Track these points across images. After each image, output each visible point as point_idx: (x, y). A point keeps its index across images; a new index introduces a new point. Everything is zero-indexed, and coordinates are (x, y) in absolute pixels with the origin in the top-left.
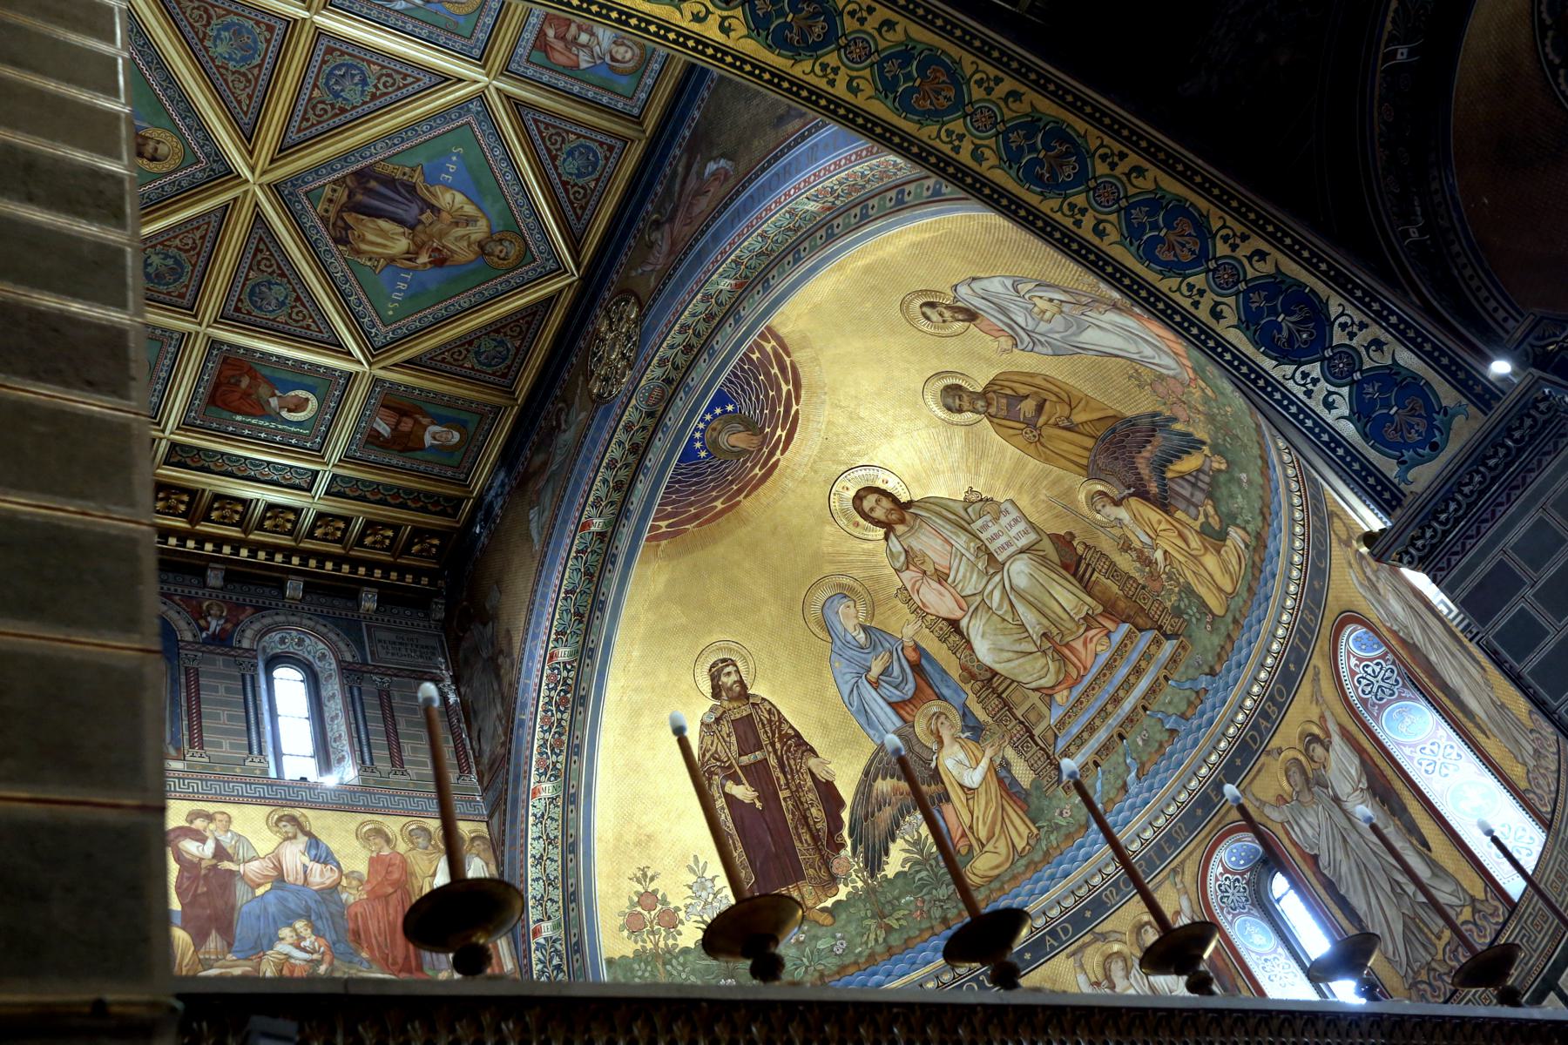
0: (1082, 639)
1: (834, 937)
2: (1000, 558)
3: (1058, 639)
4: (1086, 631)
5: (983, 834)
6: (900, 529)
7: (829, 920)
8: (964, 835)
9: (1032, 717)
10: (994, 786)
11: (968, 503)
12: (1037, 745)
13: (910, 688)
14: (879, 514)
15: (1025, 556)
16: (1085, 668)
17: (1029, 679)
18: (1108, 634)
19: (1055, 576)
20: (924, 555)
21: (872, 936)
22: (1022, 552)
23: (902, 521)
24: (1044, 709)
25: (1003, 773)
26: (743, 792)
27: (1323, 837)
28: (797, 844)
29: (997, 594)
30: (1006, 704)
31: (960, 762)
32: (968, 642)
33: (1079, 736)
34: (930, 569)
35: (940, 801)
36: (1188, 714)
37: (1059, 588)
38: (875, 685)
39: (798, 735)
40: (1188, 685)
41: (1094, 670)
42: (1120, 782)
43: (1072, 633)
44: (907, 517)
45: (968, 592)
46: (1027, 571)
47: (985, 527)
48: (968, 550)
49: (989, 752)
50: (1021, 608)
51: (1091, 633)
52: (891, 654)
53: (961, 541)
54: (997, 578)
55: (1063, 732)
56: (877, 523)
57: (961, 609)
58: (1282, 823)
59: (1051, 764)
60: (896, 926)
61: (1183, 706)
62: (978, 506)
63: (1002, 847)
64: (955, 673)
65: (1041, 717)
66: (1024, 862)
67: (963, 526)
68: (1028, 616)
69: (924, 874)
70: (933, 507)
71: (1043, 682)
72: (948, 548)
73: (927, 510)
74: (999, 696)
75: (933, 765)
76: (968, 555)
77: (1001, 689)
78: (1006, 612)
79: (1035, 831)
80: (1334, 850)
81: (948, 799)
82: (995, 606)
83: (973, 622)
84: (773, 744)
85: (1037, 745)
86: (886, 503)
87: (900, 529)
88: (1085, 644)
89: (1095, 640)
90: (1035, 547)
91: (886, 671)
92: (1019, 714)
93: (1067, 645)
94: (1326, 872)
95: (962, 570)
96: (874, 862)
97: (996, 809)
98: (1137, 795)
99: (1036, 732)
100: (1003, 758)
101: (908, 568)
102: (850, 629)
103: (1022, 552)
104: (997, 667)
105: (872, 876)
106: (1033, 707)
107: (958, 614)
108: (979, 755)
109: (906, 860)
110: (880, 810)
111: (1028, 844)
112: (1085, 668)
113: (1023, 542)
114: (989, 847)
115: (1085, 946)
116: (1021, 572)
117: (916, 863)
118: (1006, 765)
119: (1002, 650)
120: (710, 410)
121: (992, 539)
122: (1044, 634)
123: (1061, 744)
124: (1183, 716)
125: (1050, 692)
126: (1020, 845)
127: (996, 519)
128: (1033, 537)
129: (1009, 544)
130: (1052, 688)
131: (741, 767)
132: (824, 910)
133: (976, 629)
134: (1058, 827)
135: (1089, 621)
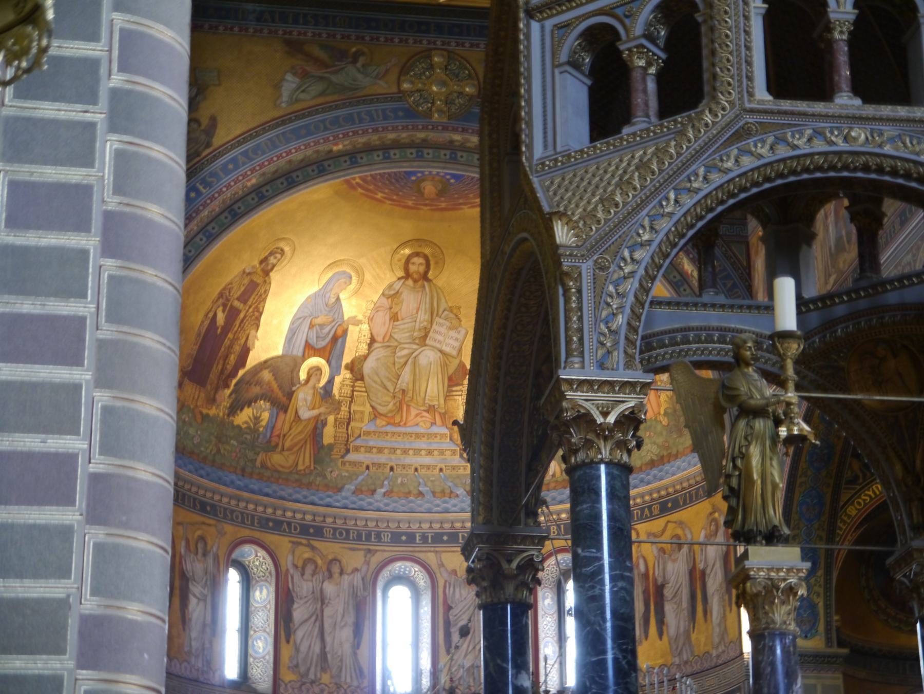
0: (418, 412)
1: (197, 432)
2: (428, 342)
3: (407, 399)
4: (424, 411)
5: (288, 444)
6: (410, 282)
7: (199, 420)
8: (279, 436)
9: (357, 416)
10: (310, 427)
12: (347, 429)
13: (322, 344)
14: (412, 268)
15: (439, 354)
16: (405, 424)
17: (374, 399)
18: (433, 424)
19: (440, 376)
20: (402, 302)
21: (211, 447)
22: (441, 351)
23: (415, 281)
24: (366, 419)
25: (319, 426)
26: (221, 318)
27: (464, 604)
28: (215, 366)
29: (405, 352)
30: (352, 397)
31: (306, 400)
32: (368, 354)
33: (371, 448)
34: (395, 310)
35: (282, 409)
36: (437, 495)
37: (436, 383)
38: (311, 326)
39: (261, 314)
40: (450, 484)
41: (409, 430)
42: (373, 487)
43: (417, 404)
44: (420, 283)
45: (396, 336)
46: (432, 359)
47: (441, 325)
48: (420, 323)
49: (322, 410)
50: (408, 369)
51: (425, 414)
52: (333, 321)
53: (423, 316)
54: (415, 347)
55: (365, 438)
56: (406, 270)
57: (384, 338)
58: (446, 581)
59: (346, 445)
60: (222, 451)
61: (438, 489)
62: (451, 315)
63: (292, 459)
64: (347, 359)
65: (362, 420)
66: (296, 476)
67: (433, 313)
68: (406, 374)
69: (249, 437)
70: (435, 295)
71: (379, 408)
72: (415, 312)
73: (431, 291)
74: (353, 391)
75: (294, 388)
76: (417, 324)
77: (357, 389)
78: (400, 363)
79: (312, 468)
80: (464, 613)
81: (286, 412)
82: (399, 354)
83: (381, 349)
84: (250, 307)
85: (347, 429)
86: (422, 269)
87: (410, 282)
88: (417, 415)
89: (424, 419)
90: (449, 358)
91: (322, 326)
92: (353, 407)
93: (408, 406)
94: (451, 617)
95: (406, 326)
96: (235, 408)
97: (300, 441)
98: (377, 501)
99: (352, 424)
100: (326, 419)
101: (388, 298)
102: (333, 292)
103: (441, 351)
104: (366, 378)
105: (229, 415)
106: (362, 412)
107: (379, 338)
108: (317, 406)
109: (246, 422)
110: (255, 385)
111: (304, 470)
112: (405, 424)
113: (447, 349)
114: (286, 453)
115: (300, 544)
116: (428, 357)
117: (249, 428)
118: (324, 424)
119: (377, 374)
120: (447, 174)
121: (436, 332)
122: (404, 391)
123: (358, 443)
124: (434, 493)
125: (378, 415)
126: (300, 467)
127: (450, 328)
128: (454, 353)
129: (440, 342)
130: (381, 414)
131: (231, 305)
132: (201, 413)
133: (379, 353)
134: (324, 477)
135: (431, 409)
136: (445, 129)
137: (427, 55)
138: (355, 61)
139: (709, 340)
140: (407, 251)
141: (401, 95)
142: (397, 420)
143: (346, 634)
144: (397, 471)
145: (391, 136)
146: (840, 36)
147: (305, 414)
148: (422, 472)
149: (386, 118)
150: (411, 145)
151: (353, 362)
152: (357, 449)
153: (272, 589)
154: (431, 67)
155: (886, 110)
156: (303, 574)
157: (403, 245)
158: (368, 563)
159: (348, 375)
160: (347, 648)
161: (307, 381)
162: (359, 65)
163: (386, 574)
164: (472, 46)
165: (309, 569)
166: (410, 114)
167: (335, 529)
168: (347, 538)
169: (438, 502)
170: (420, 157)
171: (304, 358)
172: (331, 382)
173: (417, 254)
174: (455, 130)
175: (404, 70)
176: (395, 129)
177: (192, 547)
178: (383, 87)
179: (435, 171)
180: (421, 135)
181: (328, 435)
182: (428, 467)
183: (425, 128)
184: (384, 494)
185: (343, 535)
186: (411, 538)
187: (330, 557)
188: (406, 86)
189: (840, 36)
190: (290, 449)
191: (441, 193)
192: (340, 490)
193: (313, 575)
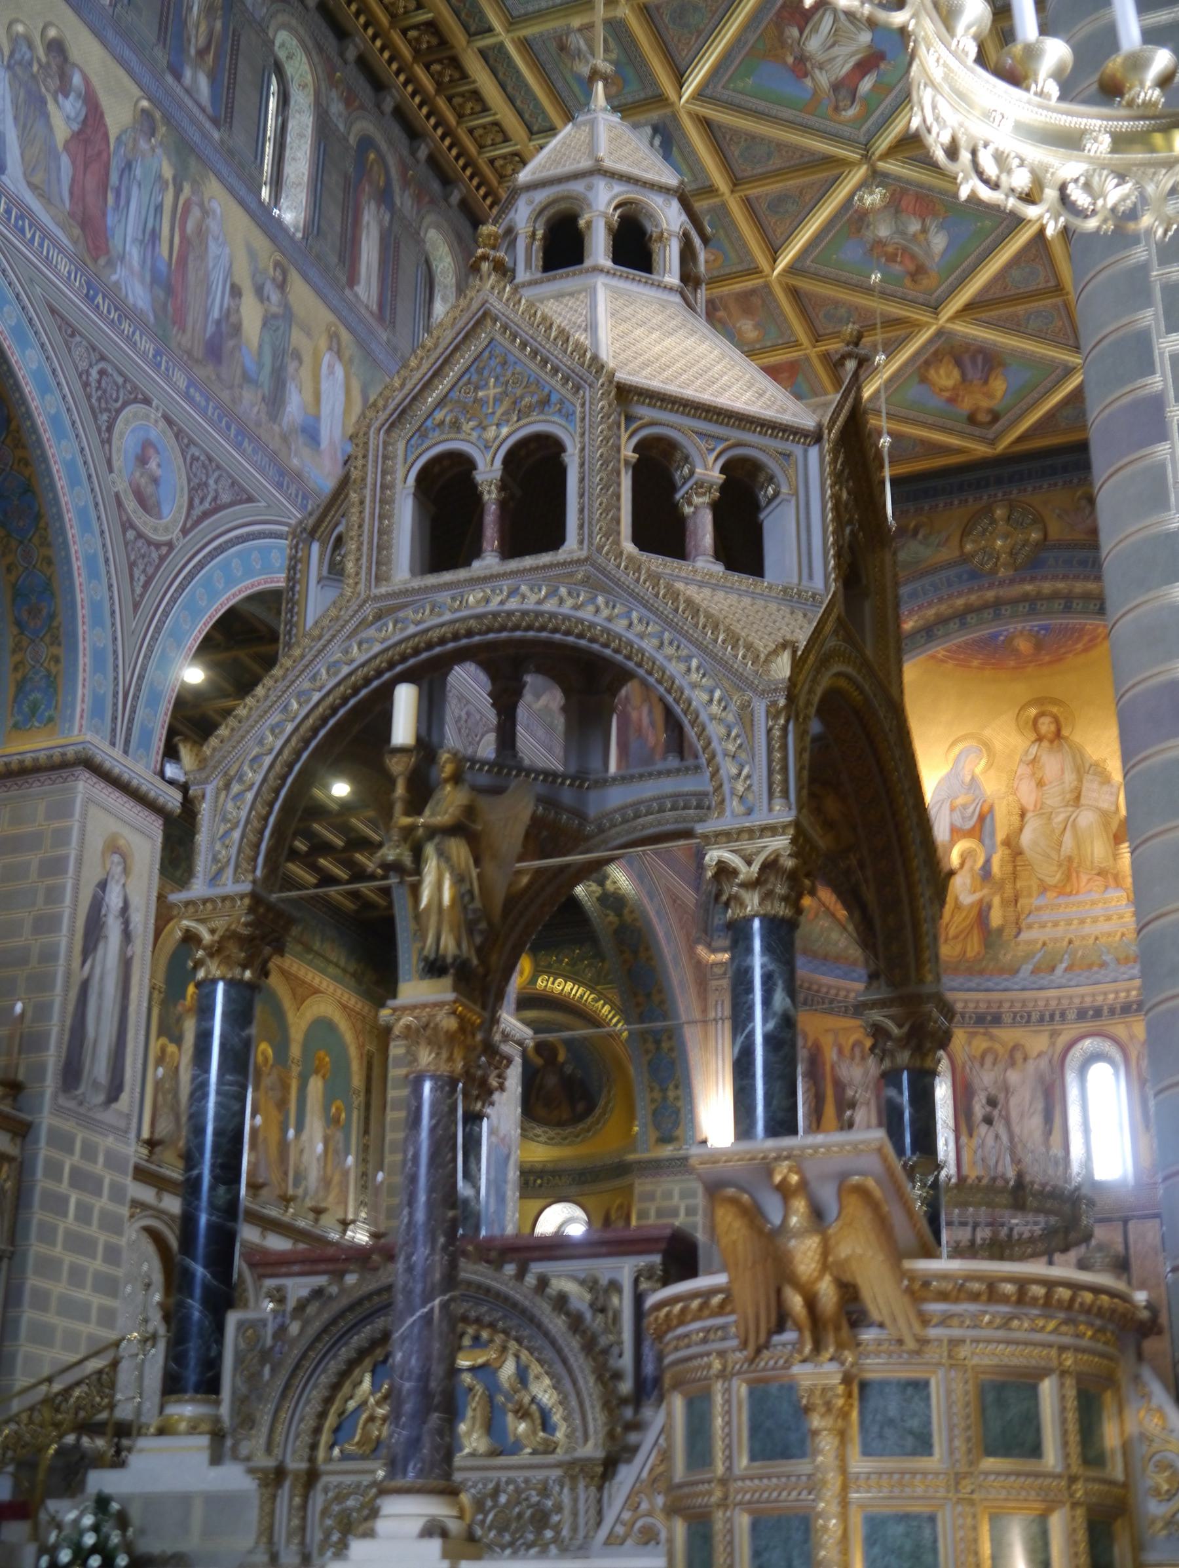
6: (1045, 744)
11: (1096, 764)
24: (1035, 894)
29: (1061, 817)
34: (1039, 775)
38: (952, 809)
50: (1068, 834)
53: (1070, 778)
63: (958, 948)
64: (1000, 836)
65: (1030, 895)
68: (1068, 841)
86: (1053, 728)
87: (1045, 744)
91: (965, 807)
93: (1078, 873)
99: (1021, 902)
107: (1030, 807)
116: (1086, 818)
118: (989, 907)
123: (1030, 920)
135: (1102, 873)
136: (1012, 581)
137: (988, 510)
138: (915, 532)
139: (661, 810)
140: (1033, 711)
141: (965, 559)
142: (1068, 890)
143: (1035, 1122)
144: (1077, 943)
145: (960, 602)
146: (491, 497)
147: (967, 899)
148: (1103, 940)
149: (950, 585)
150: (985, 606)
151: (1008, 836)
152: (1030, 927)
153: (949, 1083)
154: (993, 521)
155: (528, 561)
156: (982, 1065)
157: (1023, 708)
158: (1053, 1044)
159: (1007, 852)
160: (1038, 1135)
161: (962, 865)
162: (920, 536)
163: (1077, 1052)
164: (1035, 489)
165: (989, 1060)
166: (974, 575)
167: (1015, 1014)
168: (1028, 1021)
169: (1123, 969)
170: (997, 616)
171: (953, 843)
172: (988, 862)
173: (1042, 714)
174: (1022, 581)
175: (965, 533)
176: (960, 594)
177: (847, 1051)
178: (947, 554)
179: (1019, 626)
180: (990, 595)
181: (996, 918)
182: (1109, 935)
183: (991, 586)
184: (1066, 970)
185: (1024, 1019)
186: (1098, 1013)
187: (1011, 1044)
188: (969, 547)
189: (491, 497)
190: (956, 937)
191: (1039, 646)
192: (1017, 971)
193: (994, 1064)
